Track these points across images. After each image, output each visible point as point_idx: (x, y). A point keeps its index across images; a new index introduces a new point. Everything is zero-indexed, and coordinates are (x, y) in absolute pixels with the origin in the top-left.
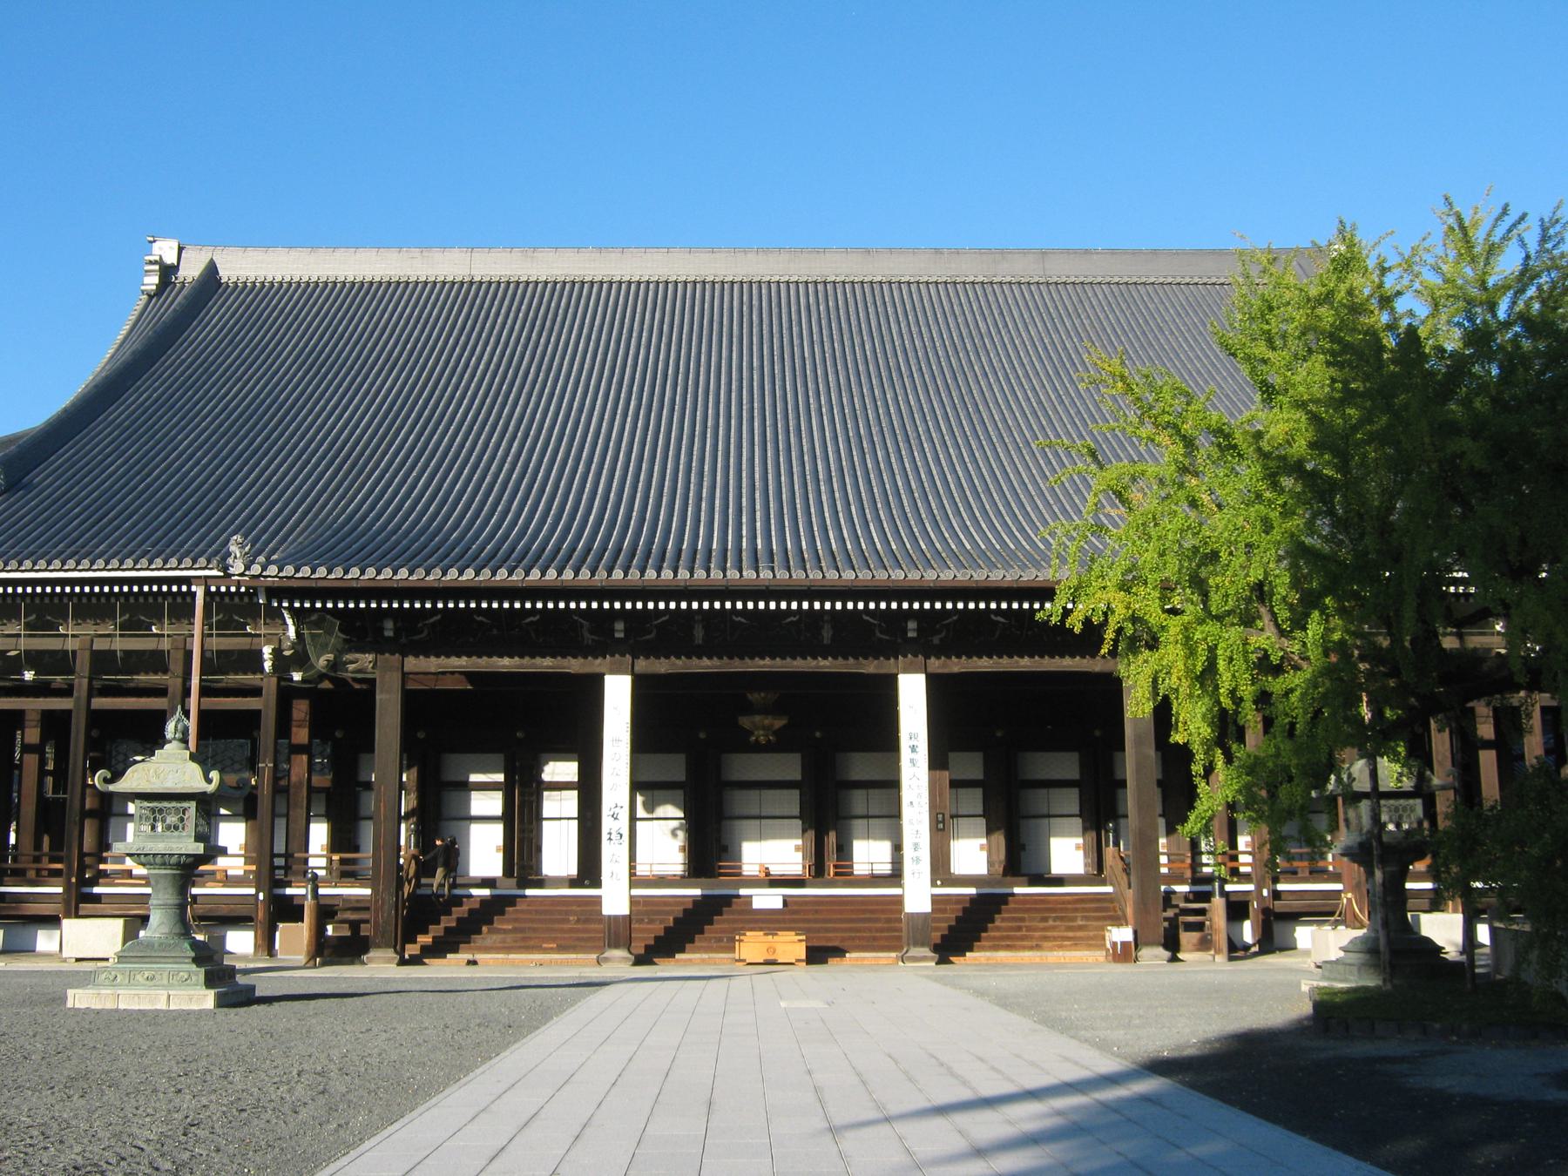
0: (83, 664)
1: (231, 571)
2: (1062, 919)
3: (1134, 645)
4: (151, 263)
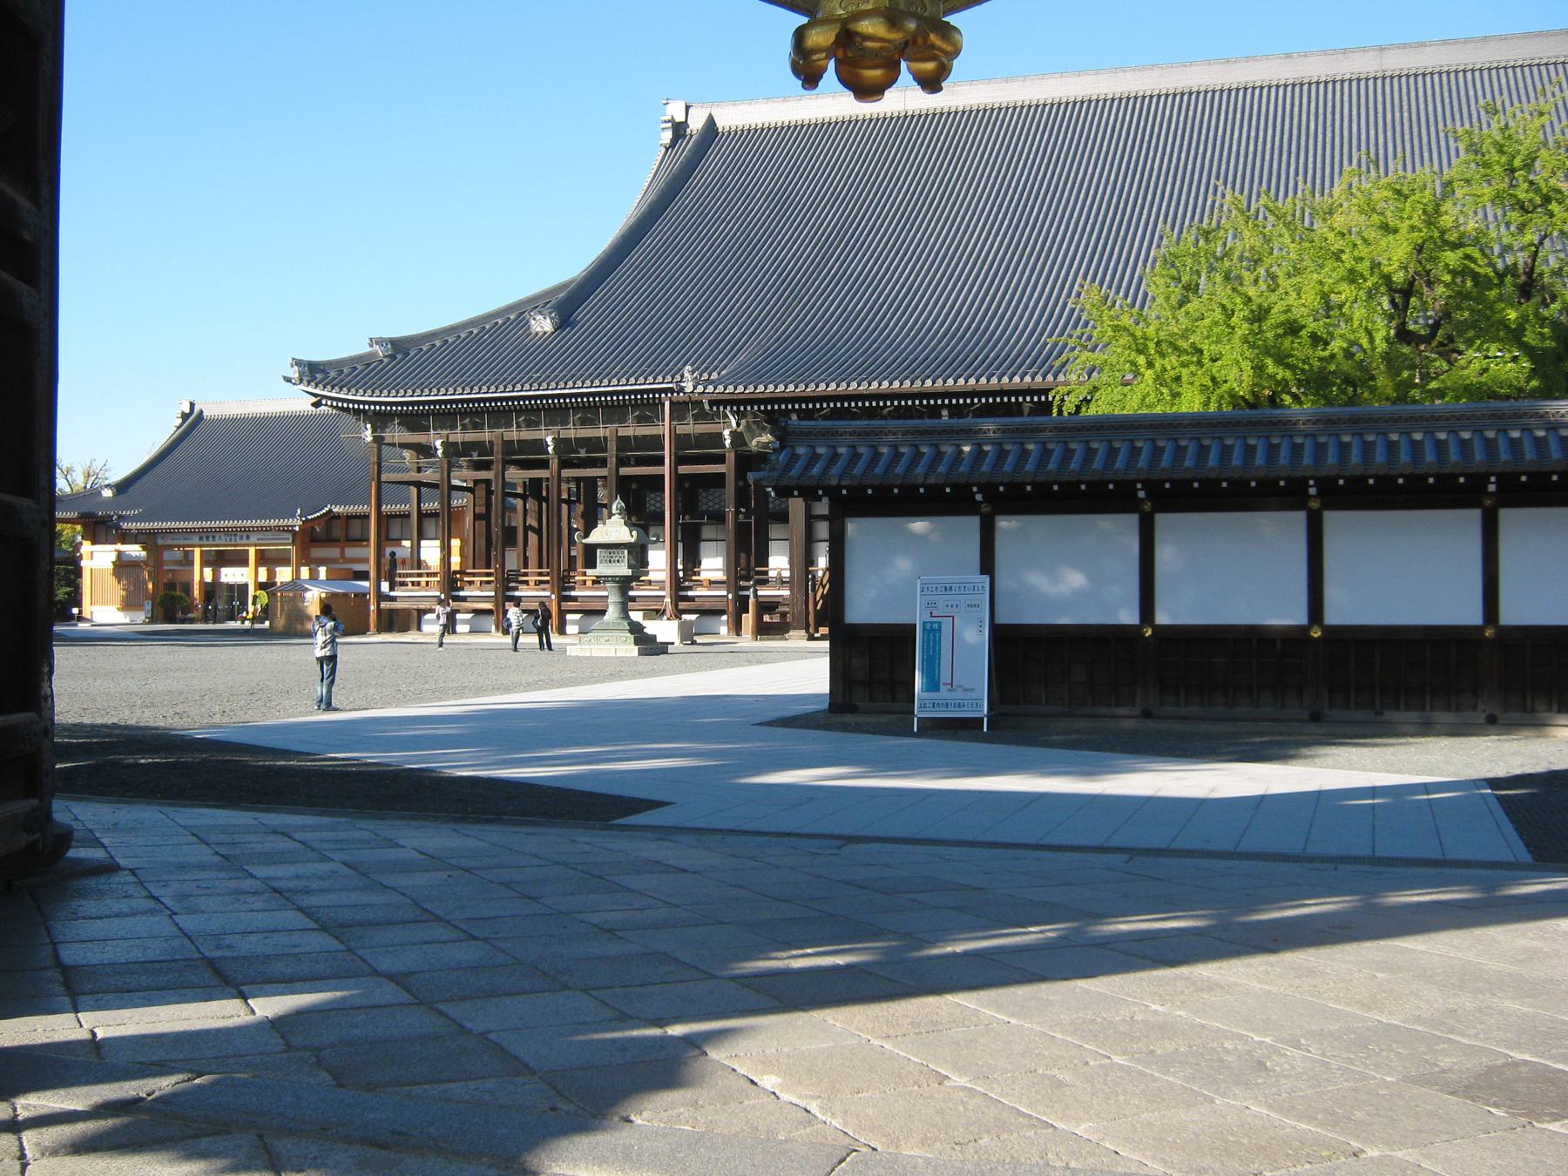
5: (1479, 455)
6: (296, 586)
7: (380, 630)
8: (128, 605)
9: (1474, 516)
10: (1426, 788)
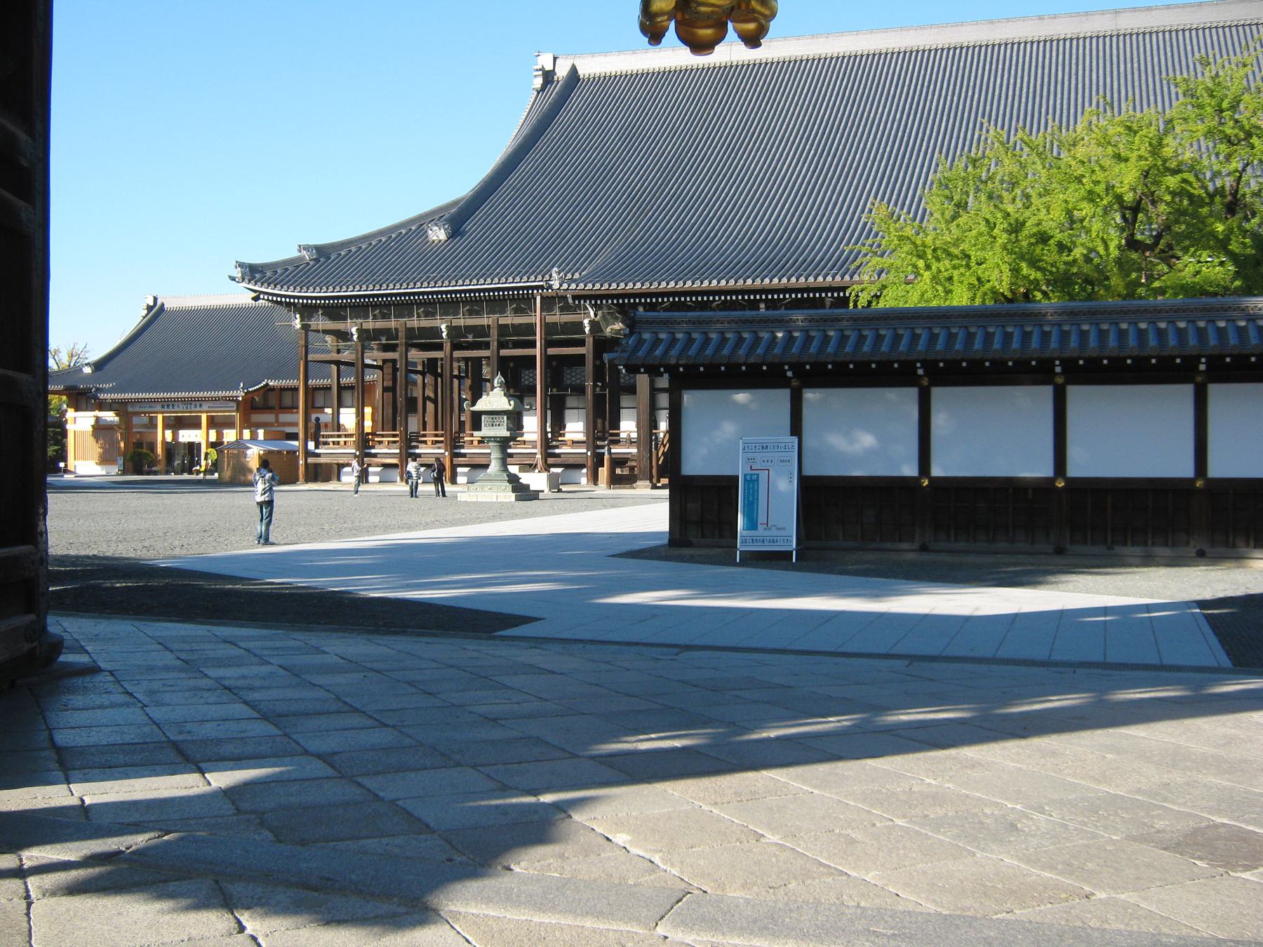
0: (494, 333)
5: (1192, 341)
6: (240, 445)
7: (307, 481)
8: (104, 460)
9: (1188, 389)
10: (1148, 608)
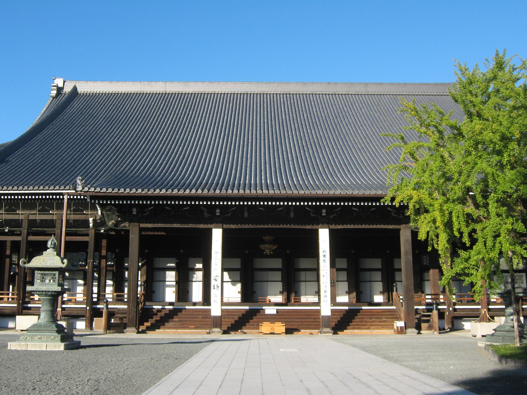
0: (25, 224)
1: (78, 189)
2: (377, 318)
3: (417, 212)
4: (54, 86)
